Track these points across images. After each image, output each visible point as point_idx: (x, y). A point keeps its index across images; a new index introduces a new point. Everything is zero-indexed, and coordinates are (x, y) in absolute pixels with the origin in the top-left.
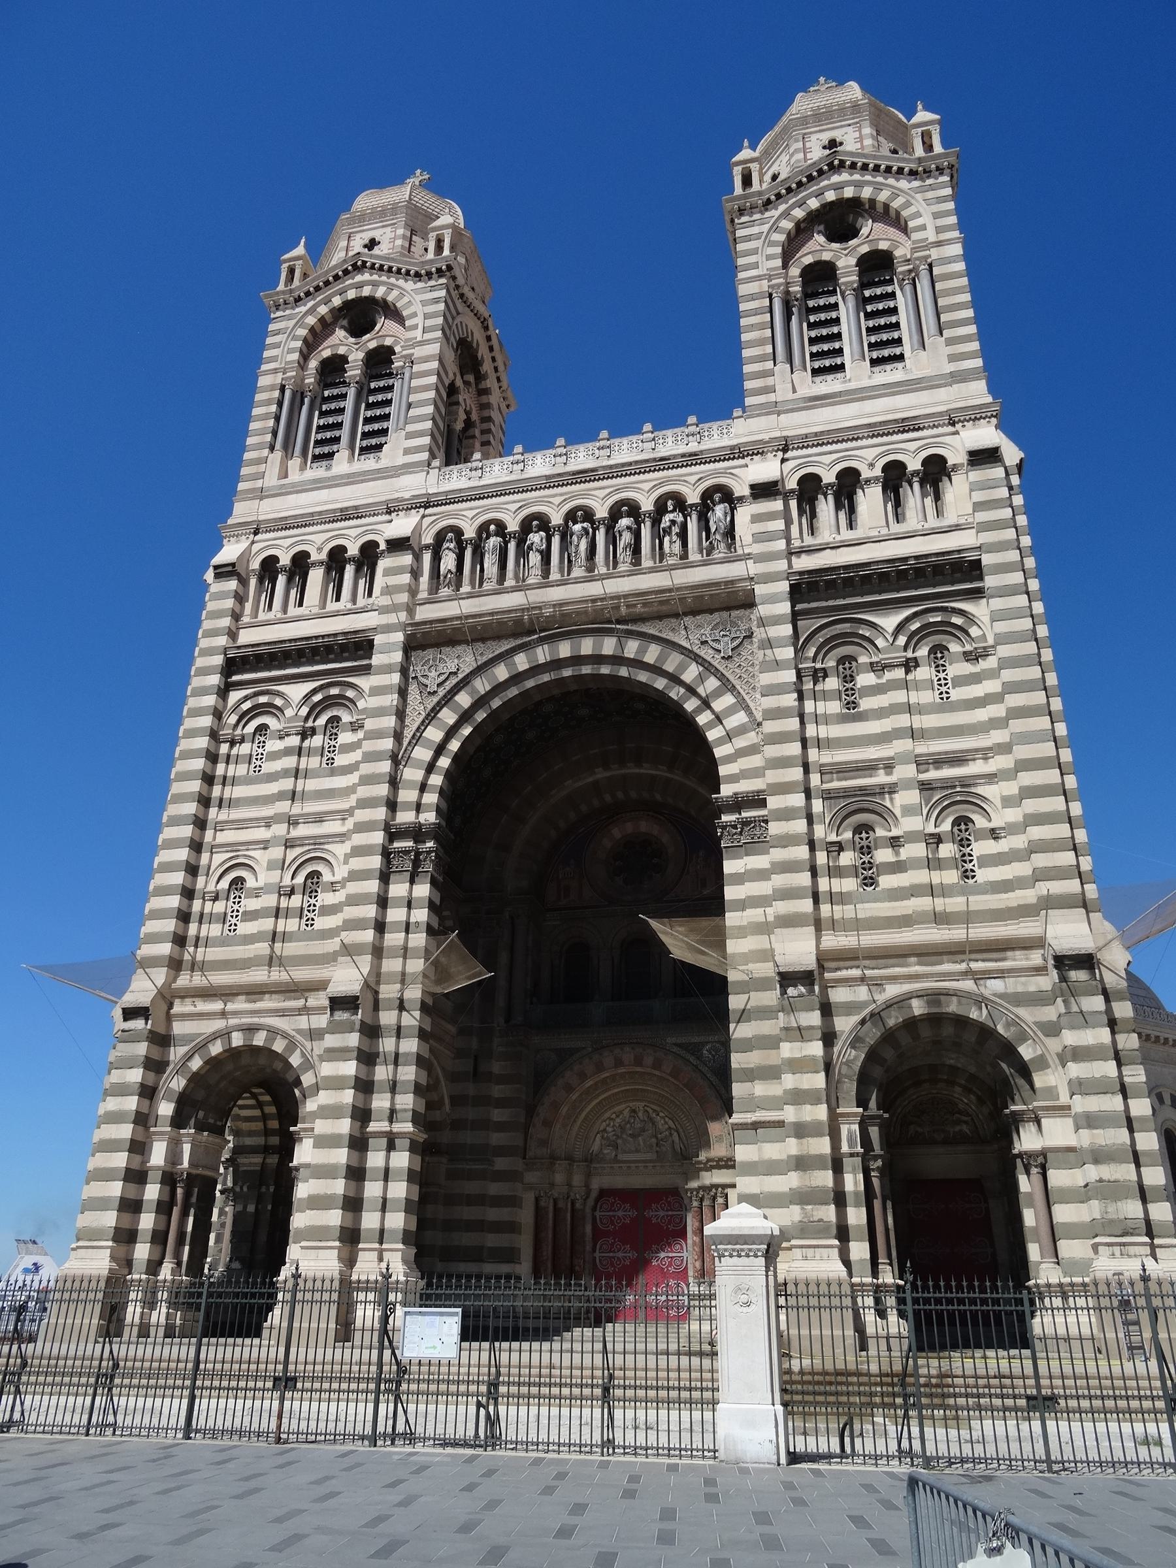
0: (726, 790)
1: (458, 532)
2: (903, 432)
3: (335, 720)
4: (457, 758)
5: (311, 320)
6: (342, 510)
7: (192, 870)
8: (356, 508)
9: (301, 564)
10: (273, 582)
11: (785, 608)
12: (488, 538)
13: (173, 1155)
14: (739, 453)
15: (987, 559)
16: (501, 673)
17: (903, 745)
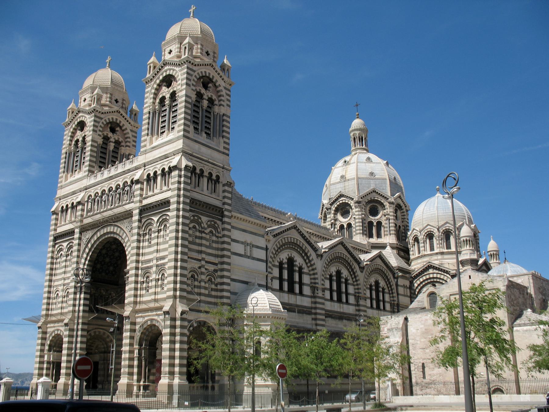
2: (166, 158)
4: (89, 261)
5: (72, 130)
6: (73, 192)
7: (49, 292)
8: (75, 191)
12: (96, 197)
13: (49, 357)
14: (137, 168)
16: (95, 238)
17: (155, 255)
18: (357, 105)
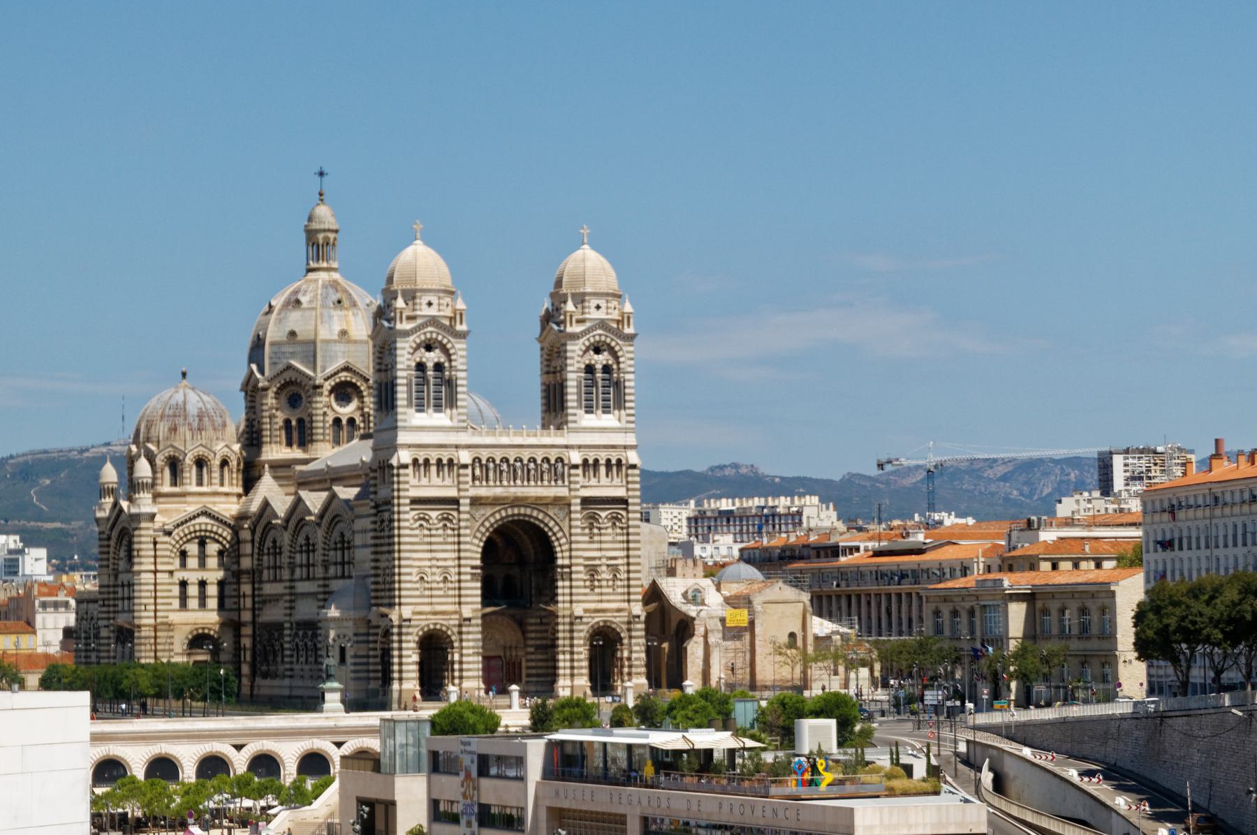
0: (560, 562)
1: (480, 461)
3: (445, 525)
9: (427, 461)
10: (419, 471)
11: (578, 508)
15: (630, 501)
16: (498, 516)
17: (603, 553)
18: (321, 174)
